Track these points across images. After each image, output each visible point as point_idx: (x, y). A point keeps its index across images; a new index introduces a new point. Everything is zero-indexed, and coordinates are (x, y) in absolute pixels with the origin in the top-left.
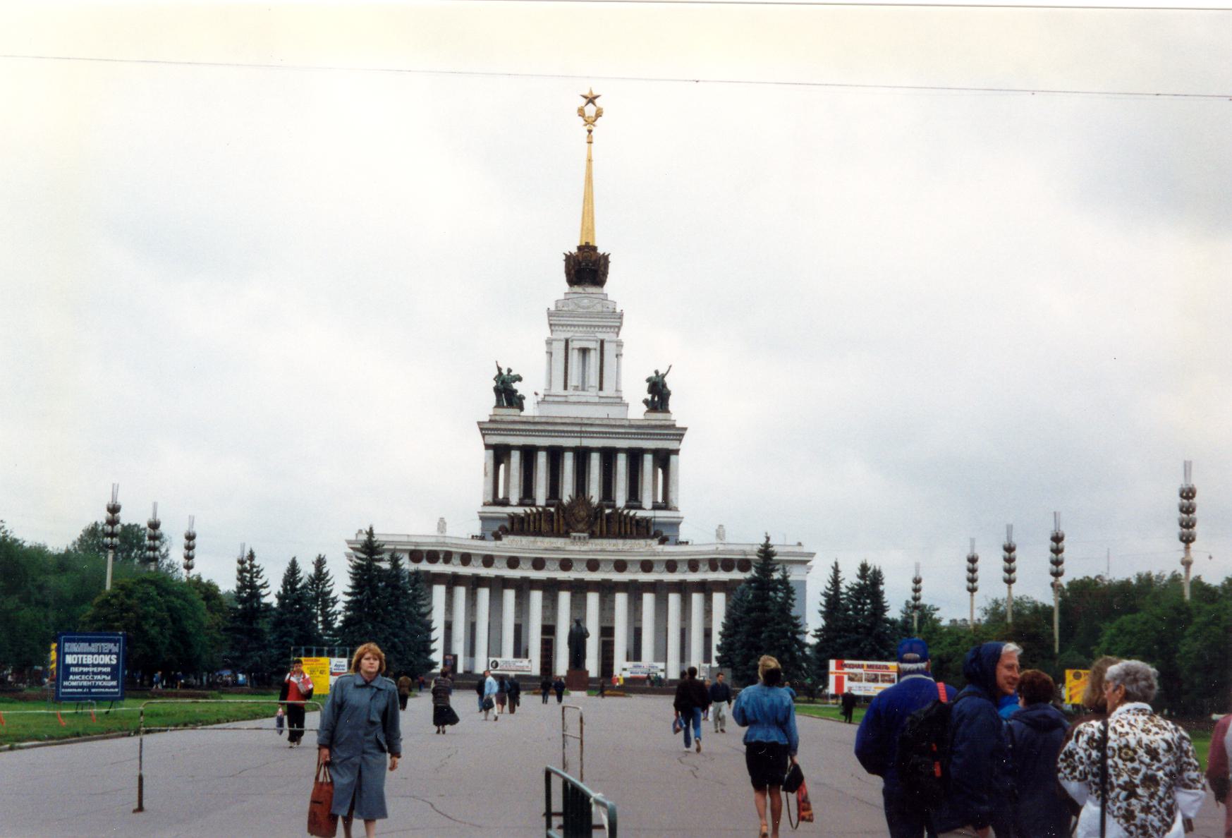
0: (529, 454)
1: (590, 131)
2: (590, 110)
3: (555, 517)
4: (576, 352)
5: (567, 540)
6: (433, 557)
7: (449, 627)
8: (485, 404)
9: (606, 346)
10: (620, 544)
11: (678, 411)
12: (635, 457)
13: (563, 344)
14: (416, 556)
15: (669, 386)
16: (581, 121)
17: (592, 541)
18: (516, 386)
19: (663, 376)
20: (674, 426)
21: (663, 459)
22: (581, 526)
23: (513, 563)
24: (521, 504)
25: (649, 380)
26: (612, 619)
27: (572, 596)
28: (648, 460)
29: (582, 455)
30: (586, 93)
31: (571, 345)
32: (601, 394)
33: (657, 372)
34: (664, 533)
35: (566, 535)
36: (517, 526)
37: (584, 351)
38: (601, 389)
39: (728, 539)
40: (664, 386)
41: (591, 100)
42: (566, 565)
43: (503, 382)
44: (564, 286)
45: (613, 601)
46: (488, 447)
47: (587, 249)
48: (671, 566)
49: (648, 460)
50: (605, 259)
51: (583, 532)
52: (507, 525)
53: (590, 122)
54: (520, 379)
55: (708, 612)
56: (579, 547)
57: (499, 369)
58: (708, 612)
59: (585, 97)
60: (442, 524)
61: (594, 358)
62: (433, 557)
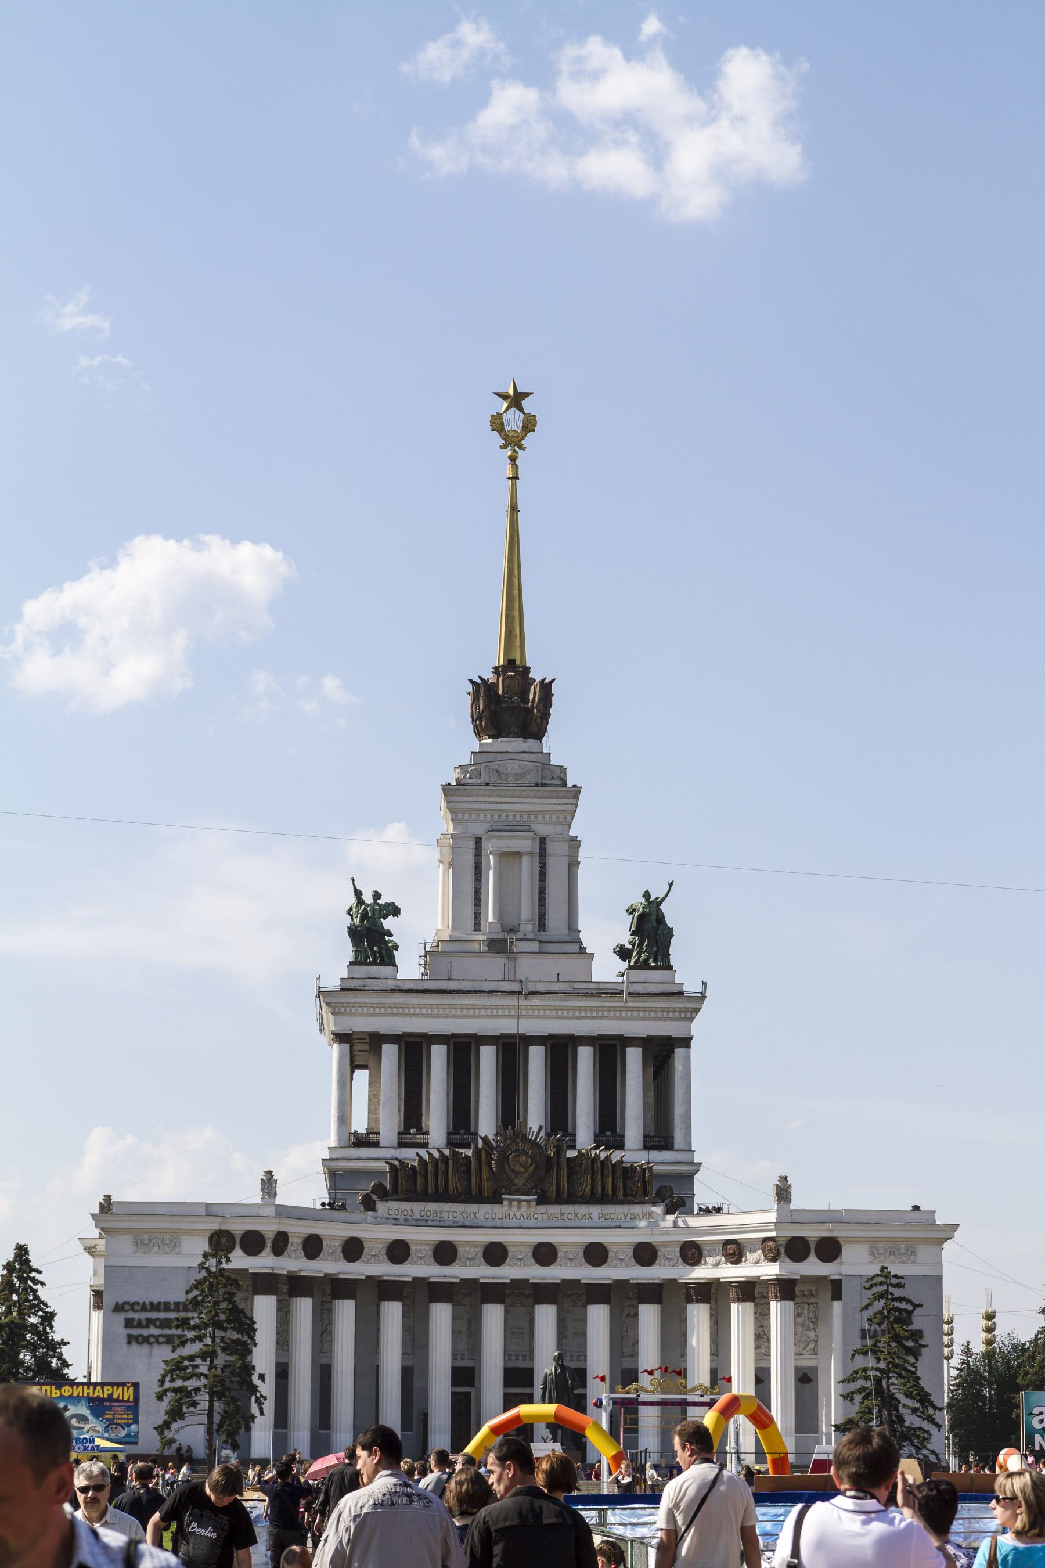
0: (414, 1050)
1: (513, 459)
2: (514, 419)
3: (474, 1166)
5: (496, 1208)
6: (253, 1243)
7: (283, 1373)
8: (335, 959)
9: (551, 848)
11: (688, 965)
12: (610, 1051)
13: (472, 844)
14: (220, 1243)
15: (669, 921)
16: (497, 440)
17: (542, 1208)
18: (388, 923)
19: (658, 903)
20: (681, 993)
21: (663, 1054)
23: (398, 1251)
24: (401, 1145)
25: (631, 911)
26: (583, 1356)
27: (506, 1312)
28: (634, 1057)
29: (512, 1050)
31: (485, 845)
32: (543, 936)
33: (647, 895)
34: (674, 1193)
35: (495, 1199)
36: (408, 1184)
38: (542, 925)
39: (798, 1202)
40: (661, 919)
41: (517, 400)
42: (495, 1254)
43: (364, 916)
44: (474, 744)
45: (584, 1320)
46: (340, 1037)
47: (514, 669)
48: (692, 1253)
49: (634, 1057)
53: (513, 442)
54: (395, 911)
55: (762, 1337)
56: (520, 1224)
57: (358, 893)
58: (762, 1337)
59: (504, 396)
60: (269, 1183)
61: (527, 867)
62: (253, 1243)
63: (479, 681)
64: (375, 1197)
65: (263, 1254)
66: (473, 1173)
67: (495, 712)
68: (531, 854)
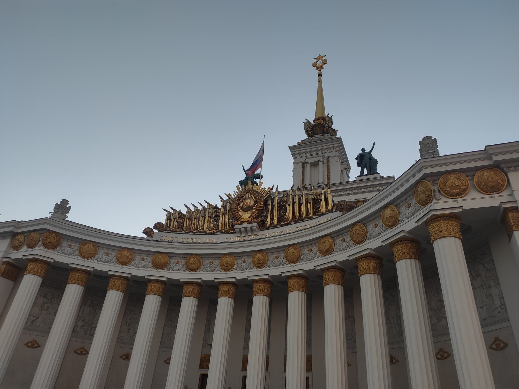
2: (320, 62)
3: (222, 212)
4: (308, 166)
9: (331, 160)
10: (294, 227)
13: (300, 165)
15: (375, 157)
16: (315, 68)
22: (246, 216)
23: (160, 261)
30: (317, 56)
35: (232, 230)
37: (315, 165)
40: (371, 158)
50: (330, 120)
51: (249, 222)
52: (163, 220)
53: (319, 68)
63: (306, 121)
64: (155, 231)
65: (37, 248)
66: (221, 215)
67: (312, 129)
68: (323, 161)
